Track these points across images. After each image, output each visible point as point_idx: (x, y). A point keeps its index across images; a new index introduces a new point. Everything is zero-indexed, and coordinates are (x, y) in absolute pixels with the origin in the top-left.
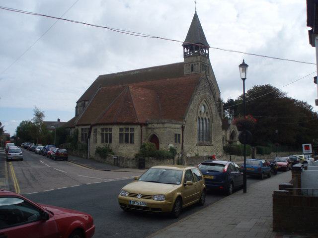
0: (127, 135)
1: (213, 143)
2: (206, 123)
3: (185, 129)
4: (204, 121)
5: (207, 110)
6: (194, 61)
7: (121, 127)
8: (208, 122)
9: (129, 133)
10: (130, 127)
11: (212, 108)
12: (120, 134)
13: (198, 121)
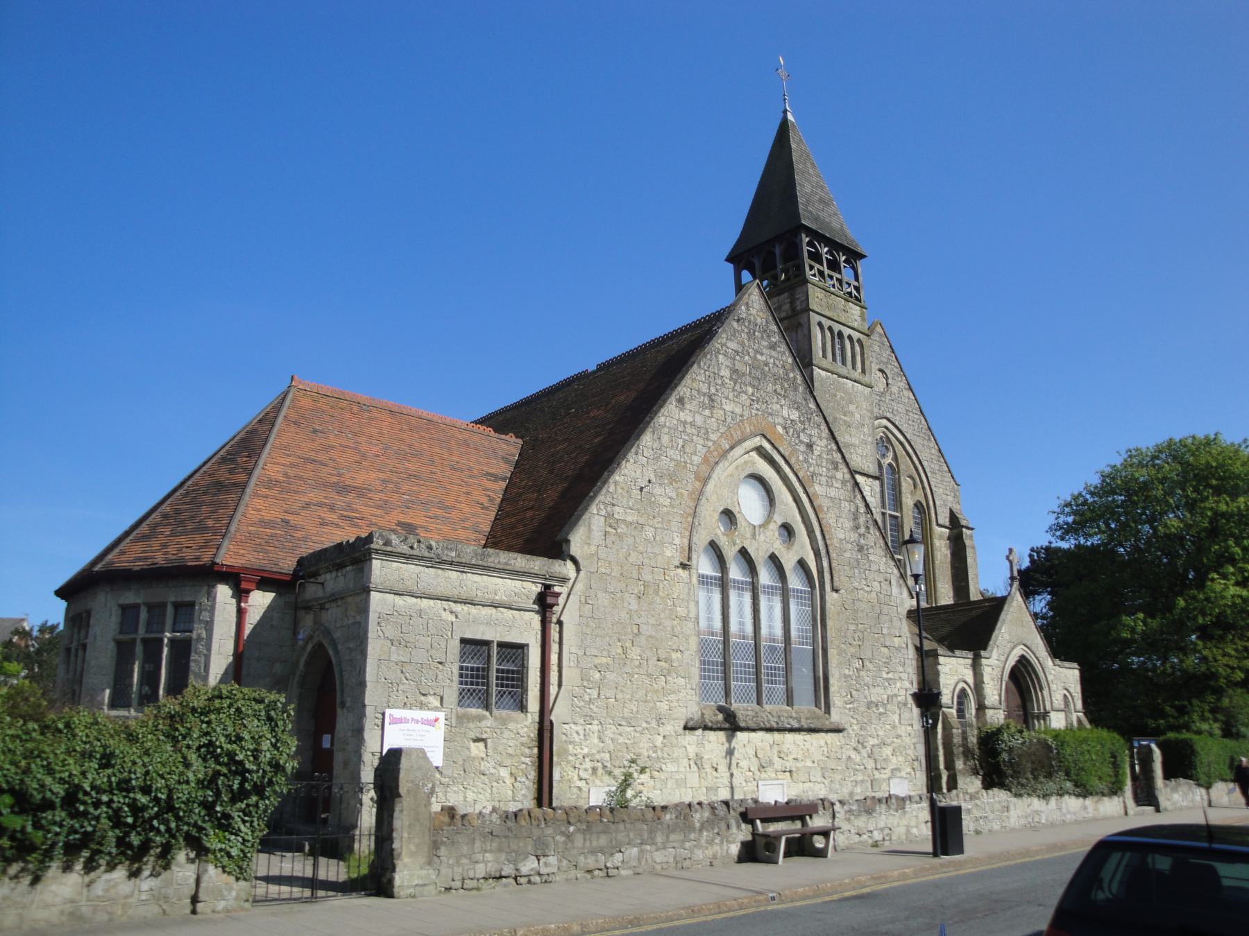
1: (836, 717)
3: (569, 612)
5: (787, 508)
11: (823, 502)
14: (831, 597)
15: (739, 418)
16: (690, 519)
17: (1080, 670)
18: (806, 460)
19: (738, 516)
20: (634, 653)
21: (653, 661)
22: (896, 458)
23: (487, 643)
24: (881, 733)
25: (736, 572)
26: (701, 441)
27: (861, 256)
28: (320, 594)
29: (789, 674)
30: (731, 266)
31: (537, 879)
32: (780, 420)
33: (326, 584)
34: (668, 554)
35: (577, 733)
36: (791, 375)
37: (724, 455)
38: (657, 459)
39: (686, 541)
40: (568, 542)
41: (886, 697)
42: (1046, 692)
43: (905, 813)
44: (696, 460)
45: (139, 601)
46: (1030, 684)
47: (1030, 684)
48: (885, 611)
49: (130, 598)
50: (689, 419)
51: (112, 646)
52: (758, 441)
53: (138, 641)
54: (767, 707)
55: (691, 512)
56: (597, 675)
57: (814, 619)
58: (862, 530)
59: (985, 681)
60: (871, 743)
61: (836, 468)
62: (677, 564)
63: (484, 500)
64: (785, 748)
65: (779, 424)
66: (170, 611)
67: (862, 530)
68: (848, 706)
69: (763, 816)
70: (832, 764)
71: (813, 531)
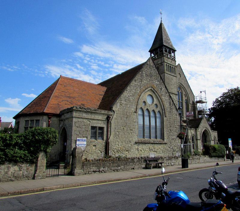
3: (113, 122)
6: (159, 63)
11: (164, 100)
12: (25, 127)
14: (165, 118)
18: (160, 92)
20: (125, 129)
21: (129, 130)
22: (182, 91)
23: (96, 127)
25: (146, 113)
28: (65, 118)
31: (103, 172)
34: (132, 110)
36: (158, 75)
37: (144, 91)
40: (112, 107)
42: (210, 137)
44: (138, 92)
49: (27, 119)
51: (24, 128)
52: (150, 88)
54: (152, 139)
58: (172, 105)
61: (167, 93)
70: (164, 150)
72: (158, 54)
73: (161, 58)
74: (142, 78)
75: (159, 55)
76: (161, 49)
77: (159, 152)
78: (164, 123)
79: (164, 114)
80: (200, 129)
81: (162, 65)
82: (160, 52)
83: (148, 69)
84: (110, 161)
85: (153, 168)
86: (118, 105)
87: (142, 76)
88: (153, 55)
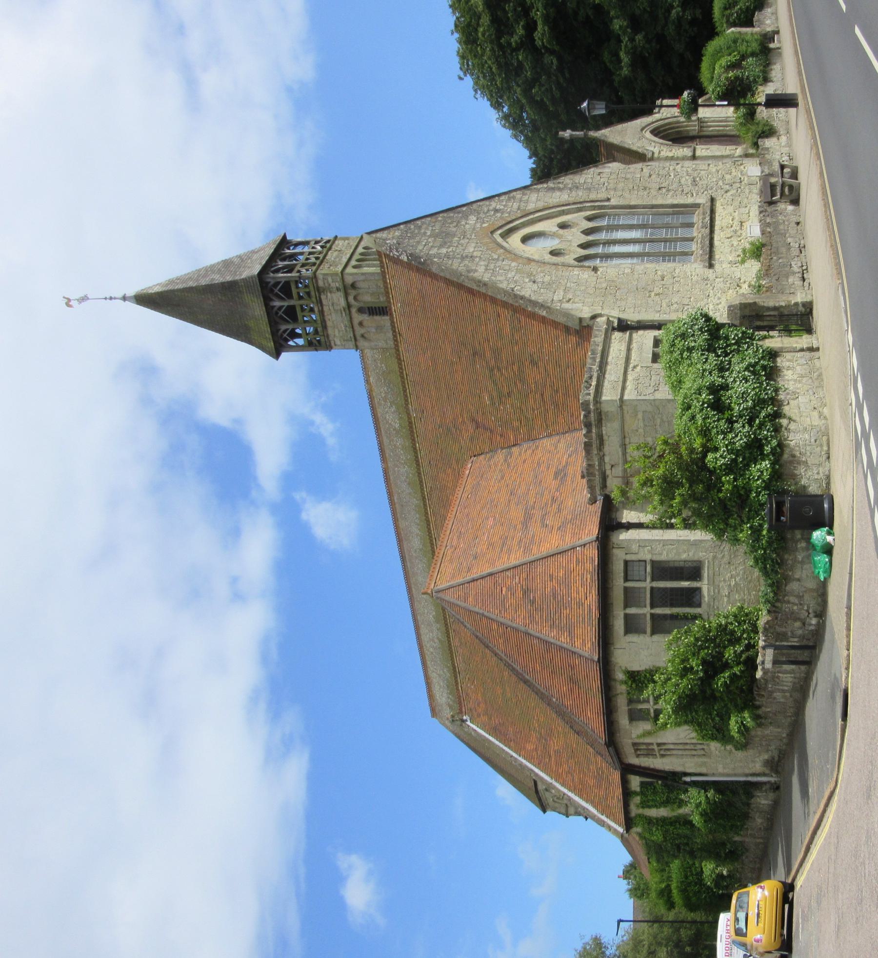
0: (659, 597)
1: (703, 200)
2: (611, 228)
3: (632, 316)
4: (603, 236)
6: (343, 303)
7: (619, 624)
8: (604, 223)
9: (648, 584)
10: (618, 584)
11: (540, 205)
13: (597, 262)
14: (613, 202)
15: (479, 244)
16: (560, 267)
17: (663, 99)
18: (509, 213)
19: (554, 248)
20: (657, 290)
21: (663, 282)
24: (715, 180)
26: (500, 262)
27: (285, 237)
29: (671, 226)
30: (284, 355)
32: (478, 225)
33: (613, 463)
35: (714, 313)
36: (440, 219)
38: (516, 282)
39: (576, 269)
40: (581, 320)
41: (687, 177)
43: (771, 148)
45: (622, 616)
46: (674, 130)
47: (674, 130)
48: (623, 176)
50: (483, 268)
53: (653, 611)
54: (695, 234)
55: (554, 267)
56: (675, 306)
57: (629, 214)
58: (561, 186)
59: (673, 155)
60: (722, 184)
61: (514, 197)
62: (593, 273)
63: (529, 452)
64: (724, 225)
65: (481, 225)
66: (629, 584)
67: (561, 186)
68: (694, 195)
69: (770, 196)
70: (736, 203)
71: (563, 211)
72: (298, 309)
73: (319, 290)
74: (459, 256)
75: (302, 302)
76: (276, 291)
77: (745, 216)
78: (633, 203)
79: (596, 204)
80: (652, 149)
81: (353, 286)
82: (289, 296)
83: (418, 242)
84: (772, 259)
85: (797, 179)
86: (570, 308)
87: (447, 256)
88: (300, 341)
